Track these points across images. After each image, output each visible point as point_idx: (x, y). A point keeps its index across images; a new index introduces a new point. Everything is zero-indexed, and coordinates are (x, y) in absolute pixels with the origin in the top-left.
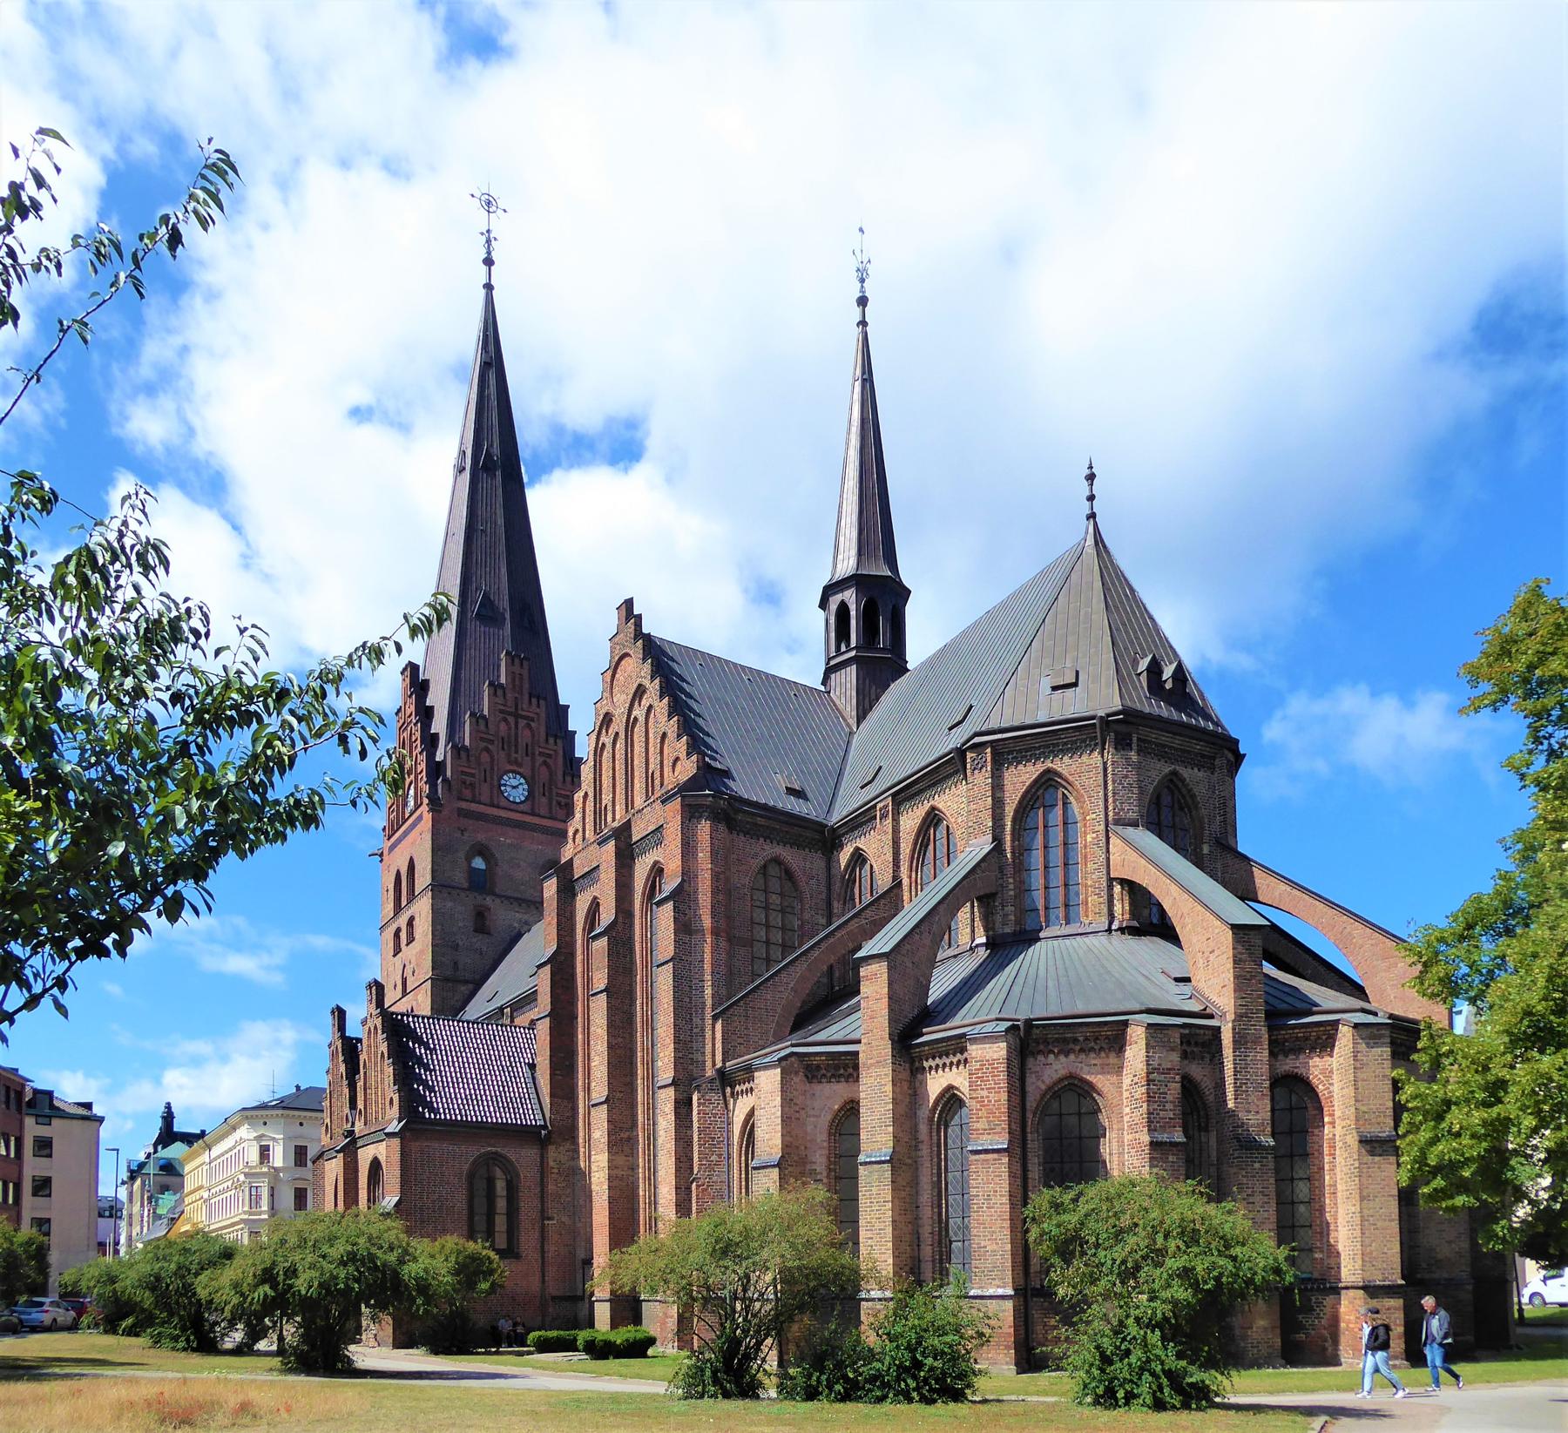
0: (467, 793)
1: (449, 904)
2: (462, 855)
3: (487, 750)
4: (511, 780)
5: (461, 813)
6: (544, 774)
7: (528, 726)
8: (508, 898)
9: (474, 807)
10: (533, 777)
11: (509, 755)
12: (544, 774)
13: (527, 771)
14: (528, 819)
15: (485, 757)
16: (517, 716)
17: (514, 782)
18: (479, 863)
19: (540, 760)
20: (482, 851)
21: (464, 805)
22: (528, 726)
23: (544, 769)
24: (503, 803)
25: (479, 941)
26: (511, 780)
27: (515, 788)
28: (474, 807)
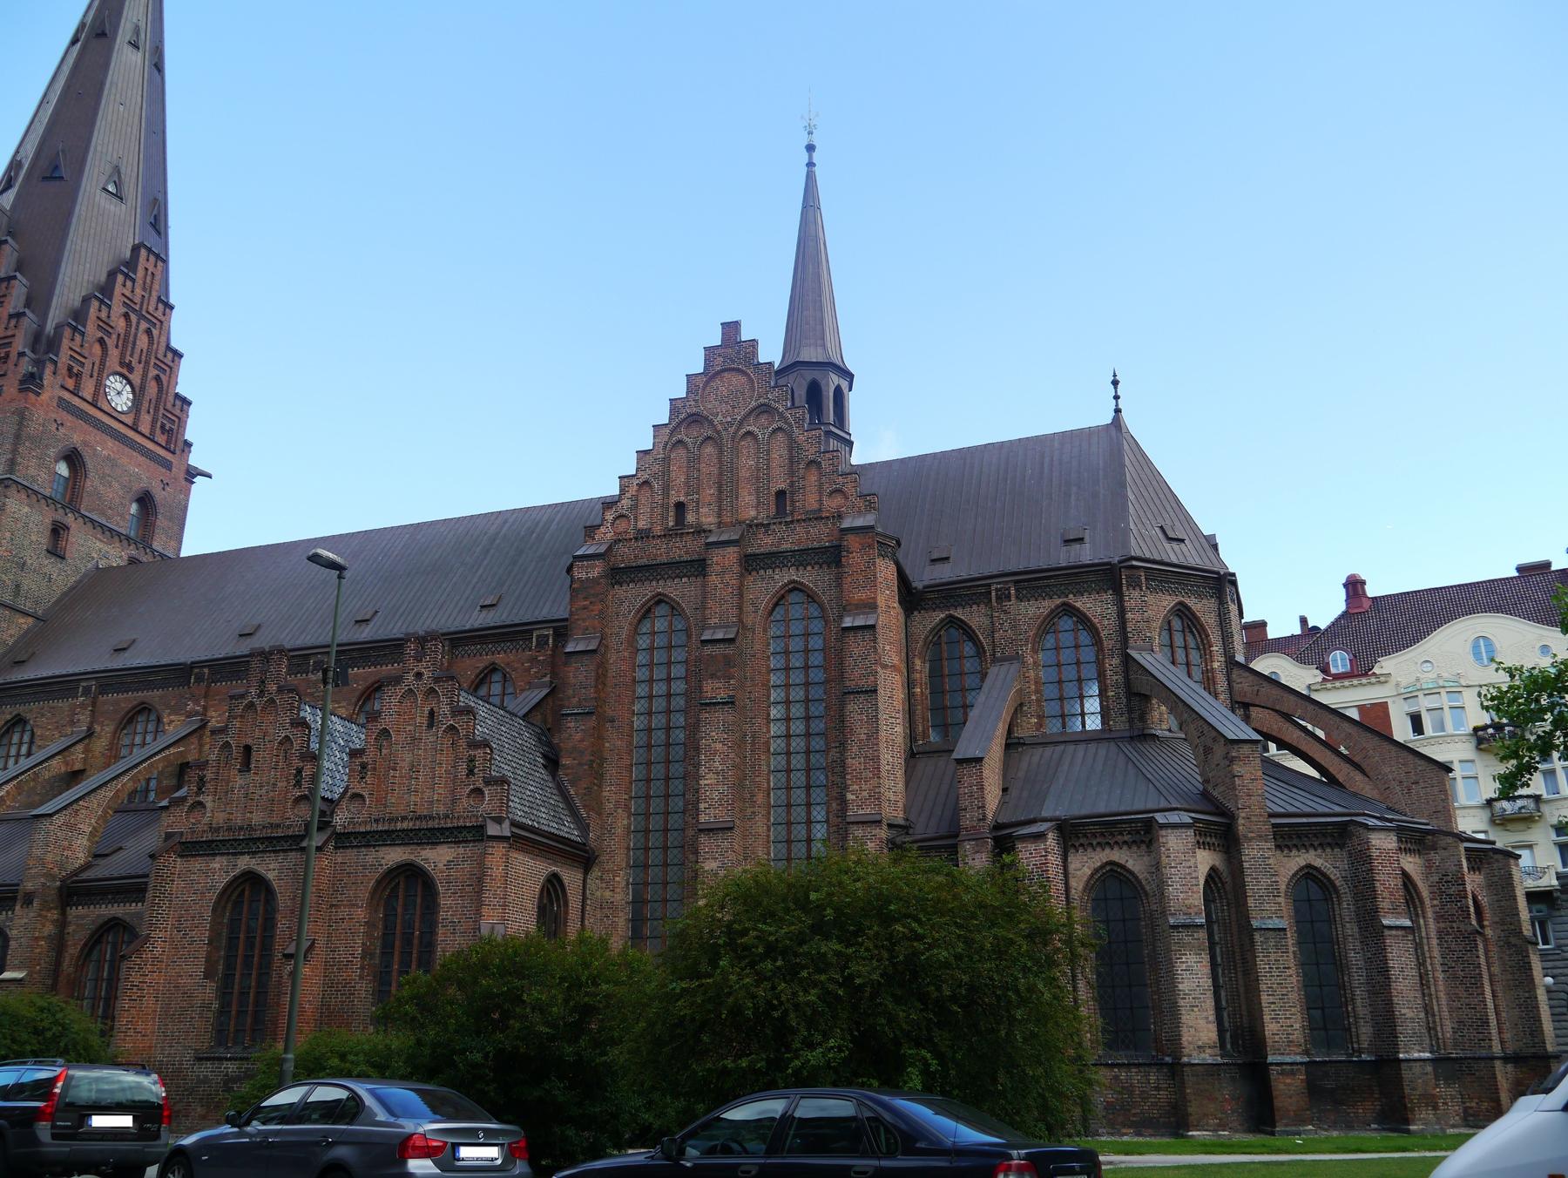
0: (70, 383)
1: (26, 509)
2: (52, 452)
3: (101, 341)
4: (114, 383)
5: (62, 404)
6: (152, 389)
7: (149, 332)
8: (92, 521)
9: (76, 401)
10: (143, 387)
11: (123, 355)
12: (152, 389)
13: (136, 378)
14: (131, 434)
15: (97, 349)
16: (141, 317)
17: (118, 386)
18: (63, 469)
19: (153, 372)
20: (73, 458)
21: (67, 396)
22: (149, 332)
23: (154, 383)
24: (106, 408)
25: (50, 566)
26: (114, 383)
27: (120, 396)
28: (76, 401)
